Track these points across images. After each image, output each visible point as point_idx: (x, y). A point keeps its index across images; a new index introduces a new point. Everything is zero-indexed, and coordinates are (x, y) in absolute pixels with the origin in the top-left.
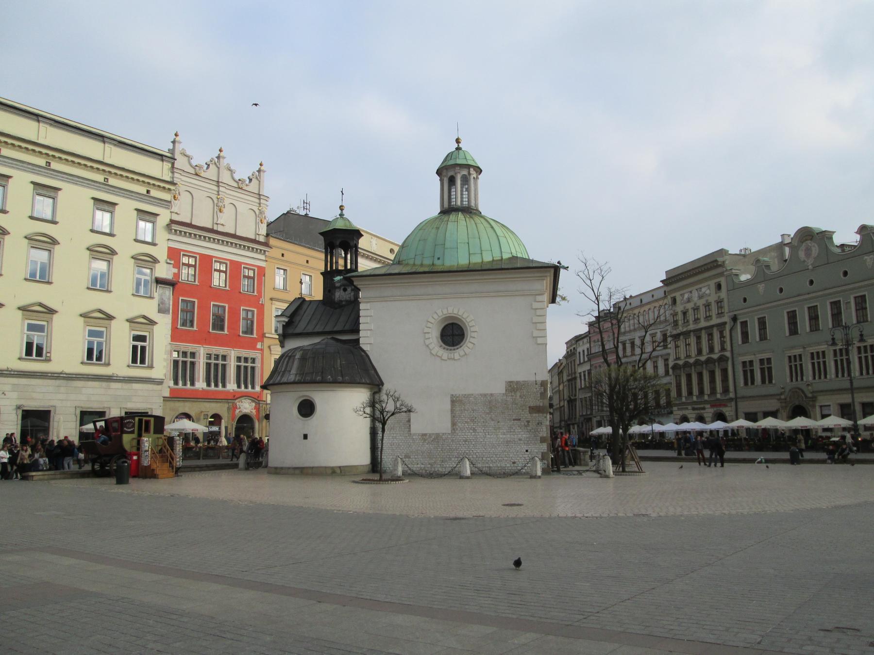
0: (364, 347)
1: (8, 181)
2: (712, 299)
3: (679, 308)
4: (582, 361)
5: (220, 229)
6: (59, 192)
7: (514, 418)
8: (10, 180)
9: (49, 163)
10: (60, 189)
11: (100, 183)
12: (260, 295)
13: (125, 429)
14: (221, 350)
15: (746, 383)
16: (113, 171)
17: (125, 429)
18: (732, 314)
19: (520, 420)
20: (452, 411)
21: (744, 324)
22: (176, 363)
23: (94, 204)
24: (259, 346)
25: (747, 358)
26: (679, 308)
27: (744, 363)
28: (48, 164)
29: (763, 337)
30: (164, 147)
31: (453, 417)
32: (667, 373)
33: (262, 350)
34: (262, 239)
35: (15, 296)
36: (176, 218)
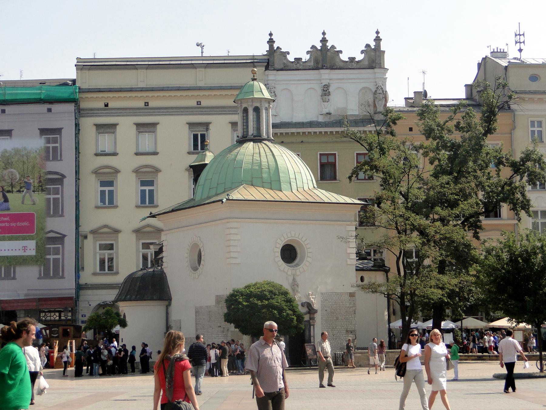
1: (116, 128)
6: (158, 125)
7: (219, 325)
8: (118, 127)
9: (148, 103)
10: (158, 124)
11: (192, 108)
13: (52, 335)
16: (201, 93)
17: (52, 335)
19: (220, 327)
20: (196, 319)
23: (189, 128)
28: (147, 104)
30: (262, 50)
31: (196, 324)
35: (129, 222)
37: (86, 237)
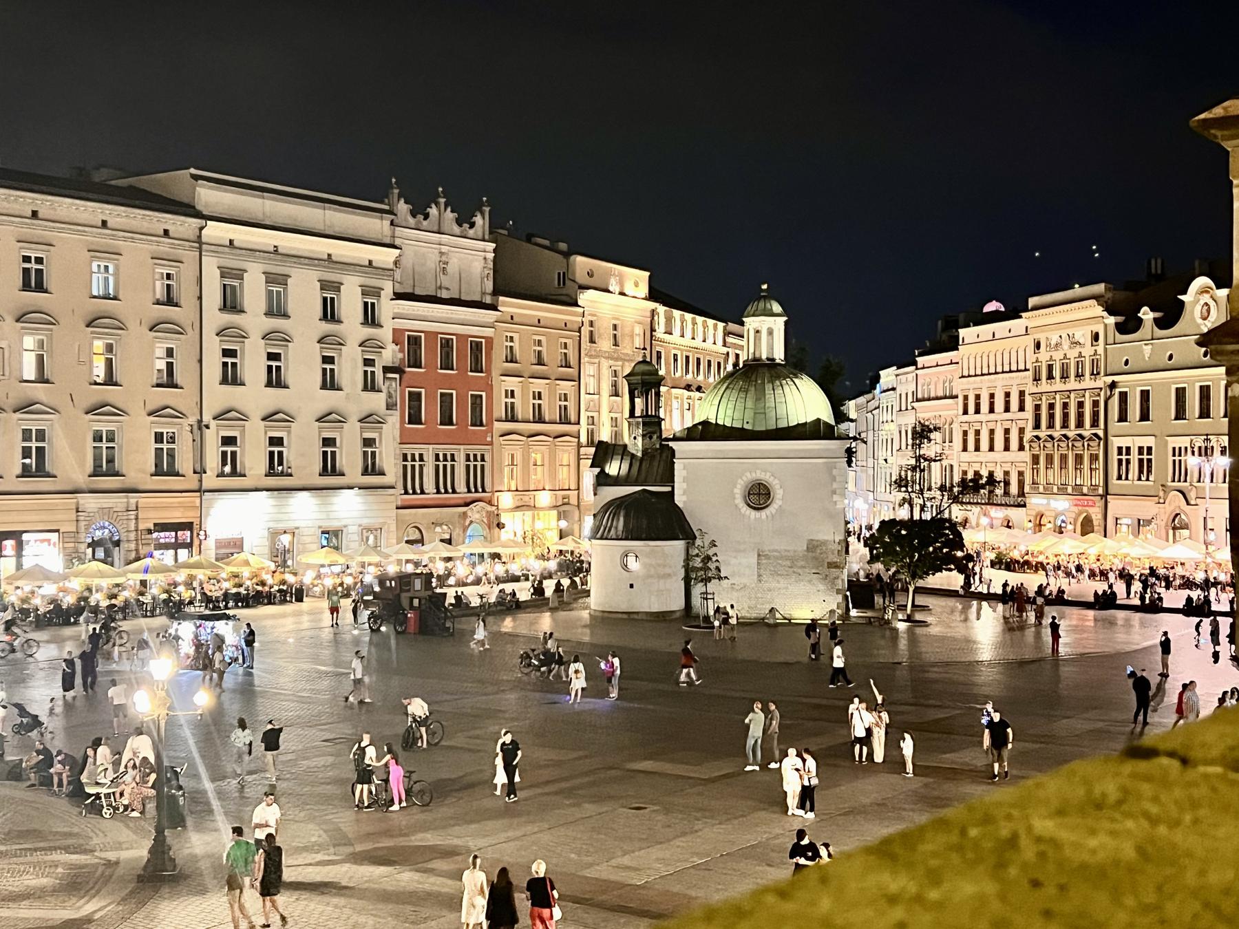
0: (680, 505)
2: (1088, 351)
3: (1044, 356)
4: (903, 408)
5: (444, 295)
12: (489, 372)
14: (449, 449)
15: (1119, 478)
18: (1109, 379)
21: (1123, 397)
22: (405, 467)
24: (489, 439)
25: (1124, 442)
26: (1044, 356)
27: (1120, 449)
29: (1145, 416)
32: (1021, 448)
33: (491, 444)
34: (488, 300)
36: (399, 290)
37: (207, 427)
